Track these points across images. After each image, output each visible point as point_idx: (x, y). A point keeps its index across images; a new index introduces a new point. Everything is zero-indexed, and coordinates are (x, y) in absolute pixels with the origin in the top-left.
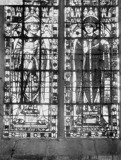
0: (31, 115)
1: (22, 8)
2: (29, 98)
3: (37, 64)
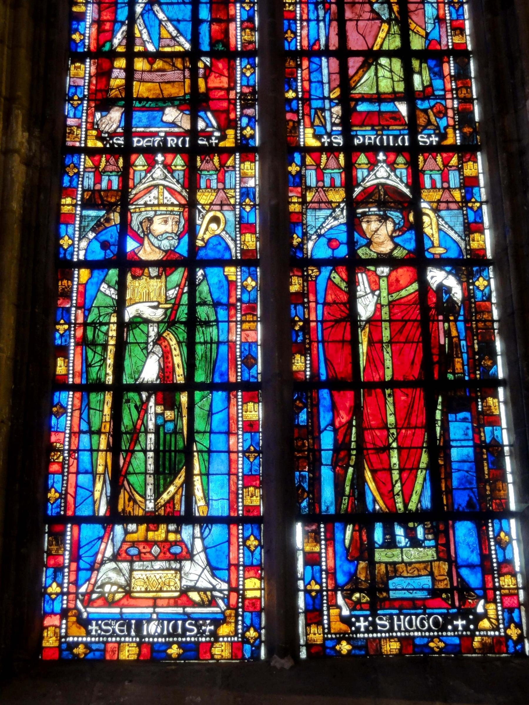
0: (158, 565)
1: (121, 161)
2: (144, 496)
3: (177, 360)
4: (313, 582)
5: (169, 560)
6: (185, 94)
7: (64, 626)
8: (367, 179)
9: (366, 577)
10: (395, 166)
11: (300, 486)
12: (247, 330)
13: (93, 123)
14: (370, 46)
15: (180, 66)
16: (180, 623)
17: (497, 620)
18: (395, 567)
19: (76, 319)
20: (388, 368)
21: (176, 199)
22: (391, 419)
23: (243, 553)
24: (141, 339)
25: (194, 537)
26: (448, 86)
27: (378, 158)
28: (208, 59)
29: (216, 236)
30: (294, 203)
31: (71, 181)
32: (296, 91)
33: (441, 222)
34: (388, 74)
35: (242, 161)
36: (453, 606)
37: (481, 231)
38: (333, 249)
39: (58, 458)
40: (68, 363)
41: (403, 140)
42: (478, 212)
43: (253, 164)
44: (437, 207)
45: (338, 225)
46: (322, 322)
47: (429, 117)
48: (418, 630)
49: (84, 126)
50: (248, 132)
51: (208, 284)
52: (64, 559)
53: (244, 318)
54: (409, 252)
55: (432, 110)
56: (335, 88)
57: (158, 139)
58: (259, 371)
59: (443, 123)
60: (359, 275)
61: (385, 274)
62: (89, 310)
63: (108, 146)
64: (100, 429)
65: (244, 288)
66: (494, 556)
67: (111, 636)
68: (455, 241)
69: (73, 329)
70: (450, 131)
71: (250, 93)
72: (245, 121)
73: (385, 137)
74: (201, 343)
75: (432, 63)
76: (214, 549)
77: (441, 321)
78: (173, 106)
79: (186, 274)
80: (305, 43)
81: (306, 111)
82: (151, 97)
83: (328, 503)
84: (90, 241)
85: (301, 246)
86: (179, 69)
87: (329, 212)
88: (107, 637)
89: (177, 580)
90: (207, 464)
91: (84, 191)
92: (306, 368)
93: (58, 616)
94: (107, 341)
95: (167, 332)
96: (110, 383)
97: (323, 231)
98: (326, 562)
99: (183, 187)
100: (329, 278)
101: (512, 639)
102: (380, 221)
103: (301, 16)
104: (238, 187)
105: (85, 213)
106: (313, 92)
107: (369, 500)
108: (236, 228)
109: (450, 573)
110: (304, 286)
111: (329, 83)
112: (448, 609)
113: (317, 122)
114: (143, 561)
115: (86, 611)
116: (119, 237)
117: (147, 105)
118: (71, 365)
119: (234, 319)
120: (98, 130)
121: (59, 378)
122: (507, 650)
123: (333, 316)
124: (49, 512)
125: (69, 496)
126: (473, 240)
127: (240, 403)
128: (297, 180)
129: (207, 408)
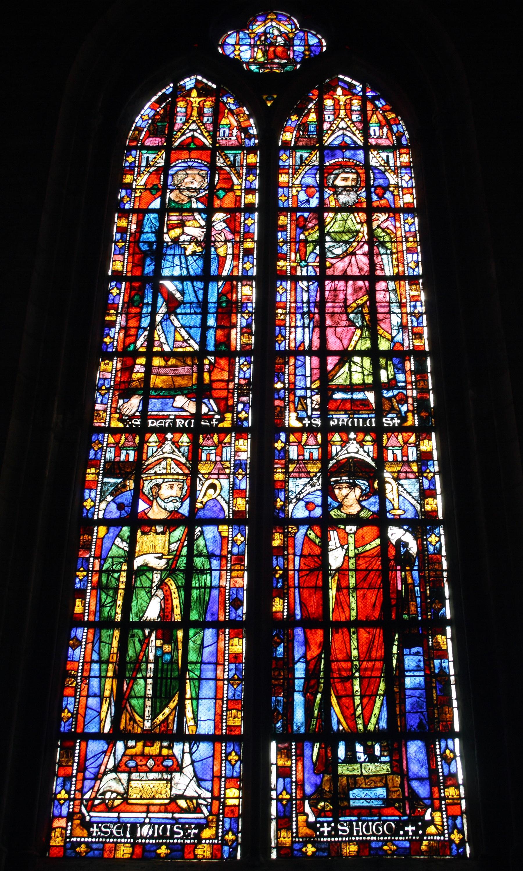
0: (152, 776)
1: (137, 438)
2: (142, 717)
3: (176, 602)
4: (284, 793)
5: (161, 772)
6: (193, 385)
7: (69, 828)
8: (340, 453)
9: (329, 788)
10: (364, 443)
11: (276, 709)
12: (235, 577)
13: (116, 408)
14: (345, 346)
15: (189, 363)
16: (169, 826)
17: (443, 826)
18: (355, 780)
19: (93, 567)
20: (353, 610)
21: (181, 469)
22: (355, 653)
23: (225, 767)
24: (147, 584)
25: (183, 753)
26: (409, 379)
27: (350, 436)
28: (213, 358)
29: (213, 499)
30: (279, 473)
31: (96, 454)
32: (283, 383)
33: (401, 489)
34: (360, 370)
35: (237, 439)
36: (404, 814)
37: (434, 496)
38: (310, 511)
39: (72, 683)
40: (85, 603)
41: (371, 422)
42: (432, 481)
43: (246, 441)
44: (398, 476)
45: (315, 491)
46: (298, 571)
47: (392, 403)
48: (373, 835)
49: (109, 410)
50: (243, 415)
51: (204, 539)
52: (73, 770)
53: (233, 567)
54: (374, 513)
55: (395, 398)
56: (315, 381)
57: (169, 421)
58: (245, 611)
59: (404, 408)
60: (331, 532)
61: (352, 531)
62: (105, 560)
63: (128, 426)
64: (109, 659)
65: (234, 542)
66: (440, 770)
67: (109, 837)
68: (412, 505)
69: (90, 575)
70: (410, 415)
71: (245, 384)
72: (240, 406)
73: (356, 420)
74: (196, 588)
75: (396, 361)
76: (200, 763)
77: (399, 570)
78: (182, 394)
79: (186, 530)
80: (292, 345)
81: (292, 399)
82: (165, 387)
83: (299, 724)
84: (109, 503)
85: (283, 509)
86: (188, 365)
87: (307, 480)
88: (106, 838)
89: (168, 789)
90: (197, 690)
91: (106, 462)
92: (284, 609)
93: (65, 820)
94: (118, 585)
95: (168, 579)
96: (119, 620)
97: (302, 496)
98: (296, 774)
99: (187, 459)
100: (306, 535)
101: (456, 844)
102: (350, 488)
103: (290, 324)
104: (232, 459)
105: (105, 480)
106: (297, 383)
107: (334, 721)
108: (229, 493)
109: (402, 785)
110: (284, 541)
111: (311, 376)
112: (400, 817)
113: (300, 407)
114: (140, 772)
115: (89, 815)
116: (132, 500)
117: (161, 394)
118: (87, 605)
119: (225, 568)
120: (120, 413)
121: (77, 615)
122: (451, 853)
123: (308, 566)
124: (62, 729)
125: (79, 715)
126: (427, 504)
127: (227, 639)
128: (282, 454)
129: (199, 642)
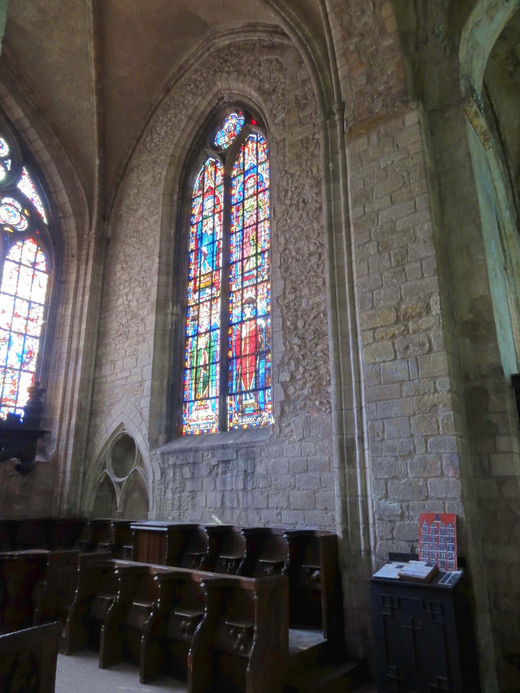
22: (248, 365)
